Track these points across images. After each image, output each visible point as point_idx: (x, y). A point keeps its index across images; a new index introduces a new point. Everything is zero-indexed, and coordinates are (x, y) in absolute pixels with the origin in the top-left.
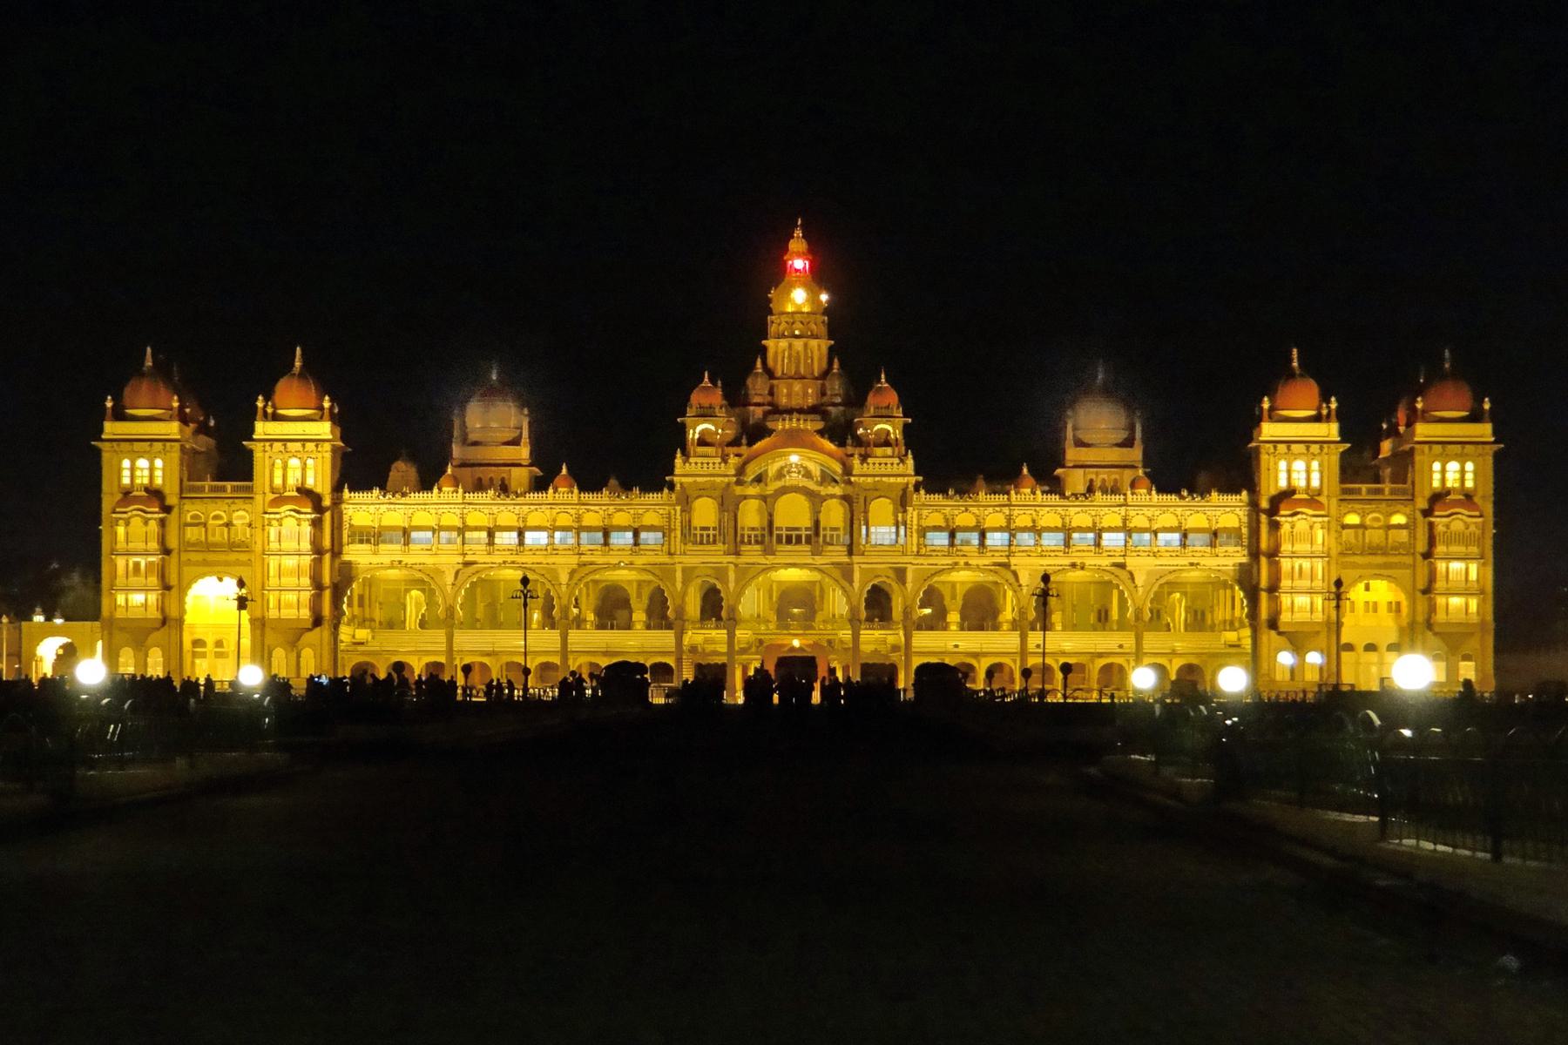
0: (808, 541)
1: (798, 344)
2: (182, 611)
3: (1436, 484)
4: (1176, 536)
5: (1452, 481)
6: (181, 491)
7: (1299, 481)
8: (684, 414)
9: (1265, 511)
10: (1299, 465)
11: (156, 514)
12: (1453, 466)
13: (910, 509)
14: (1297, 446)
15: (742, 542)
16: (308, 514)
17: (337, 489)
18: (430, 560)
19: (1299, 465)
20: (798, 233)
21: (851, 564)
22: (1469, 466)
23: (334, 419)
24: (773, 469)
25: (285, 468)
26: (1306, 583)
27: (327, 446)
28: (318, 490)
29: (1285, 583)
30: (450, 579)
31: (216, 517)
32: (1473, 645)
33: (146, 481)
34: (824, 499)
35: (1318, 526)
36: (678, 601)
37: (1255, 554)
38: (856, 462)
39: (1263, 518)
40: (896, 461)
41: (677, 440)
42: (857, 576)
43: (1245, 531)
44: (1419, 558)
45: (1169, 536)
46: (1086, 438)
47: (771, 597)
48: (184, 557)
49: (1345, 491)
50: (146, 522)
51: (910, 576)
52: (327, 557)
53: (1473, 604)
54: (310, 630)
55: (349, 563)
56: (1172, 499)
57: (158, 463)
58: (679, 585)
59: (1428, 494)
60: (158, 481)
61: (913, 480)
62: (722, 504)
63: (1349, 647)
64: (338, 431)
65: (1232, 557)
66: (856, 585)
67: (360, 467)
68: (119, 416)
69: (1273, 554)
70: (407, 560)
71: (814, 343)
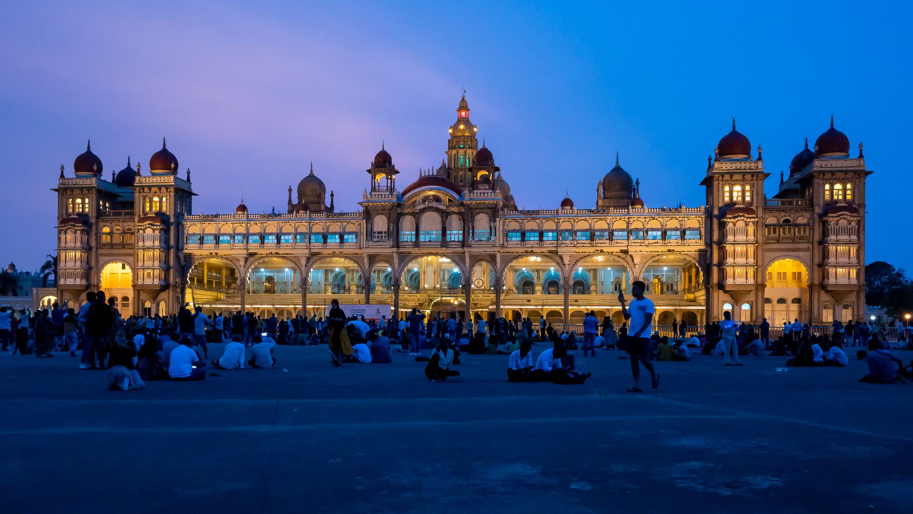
2: (99, 281)
4: (659, 233)
7: (737, 196)
9: (716, 216)
11: (80, 226)
12: (838, 186)
16: (158, 225)
18: (230, 252)
19: (737, 188)
21: (464, 253)
24: (419, 198)
25: (151, 202)
26: (741, 260)
29: (730, 260)
30: (242, 263)
31: (118, 230)
32: (852, 298)
35: (751, 224)
37: (709, 244)
39: (715, 221)
43: (703, 230)
44: (816, 244)
45: (654, 233)
48: (100, 251)
51: (498, 260)
53: (853, 272)
55: (190, 254)
57: (87, 201)
58: (367, 266)
62: (389, 220)
63: (768, 301)
65: (694, 245)
69: (721, 243)
70: (220, 252)
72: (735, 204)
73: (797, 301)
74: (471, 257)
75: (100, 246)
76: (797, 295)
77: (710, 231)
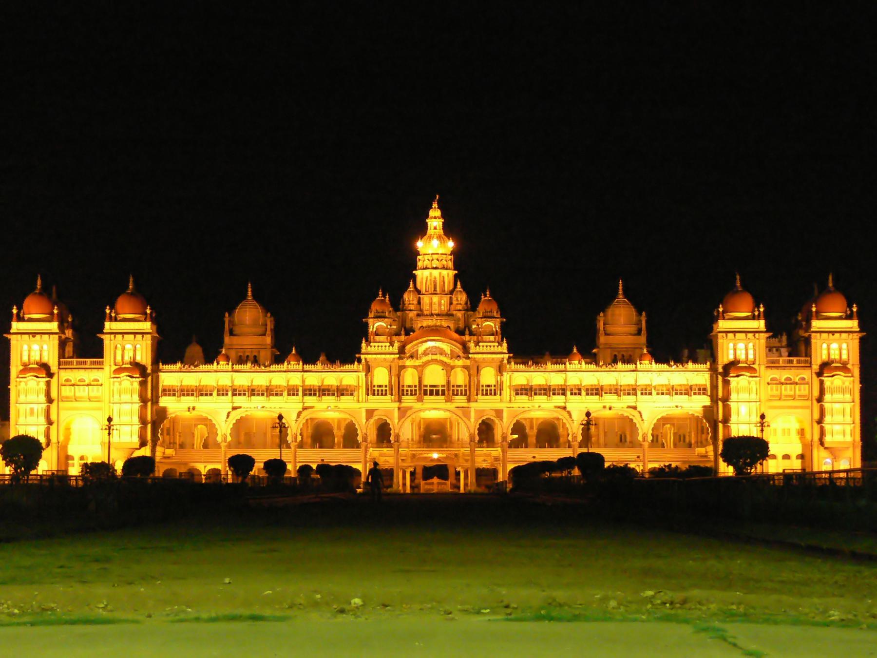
0: (443, 394)
1: (436, 273)
3: (825, 357)
5: (835, 355)
6: (59, 365)
7: (742, 356)
8: (367, 316)
9: (720, 374)
10: (741, 346)
12: (834, 346)
13: (505, 374)
14: (740, 333)
15: (403, 395)
17: (155, 361)
20: (435, 205)
22: (844, 346)
23: (154, 321)
25: (123, 350)
27: (149, 336)
28: (144, 362)
33: (38, 359)
34: (453, 368)
36: (364, 431)
37: (714, 399)
38: (472, 345)
40: (497, 344)
41: (363, 333)
42: (473, 414)
44: (815, 402)
46: (610, 329)
47: (420, 428)
49: (768, 362)
50: (38, 383)
51: (505, 415)
52: (149, 404)
54: (139, 449)
56: (664, 367)
57: (45, 347)
58: (364, 420)
59: (819, 362)
60: (45, 360)
61: (507, 356)
64: (155, 327)
66: (472, 420)
67: (168, 351)
68: (20, 319)
69: (726, 399)
71: (445, 272)
72: (739, 362)
73: (798, 457)
74: (476, 411)
75: (62, 399)
76: (799, 451)
77: (714, 387)
